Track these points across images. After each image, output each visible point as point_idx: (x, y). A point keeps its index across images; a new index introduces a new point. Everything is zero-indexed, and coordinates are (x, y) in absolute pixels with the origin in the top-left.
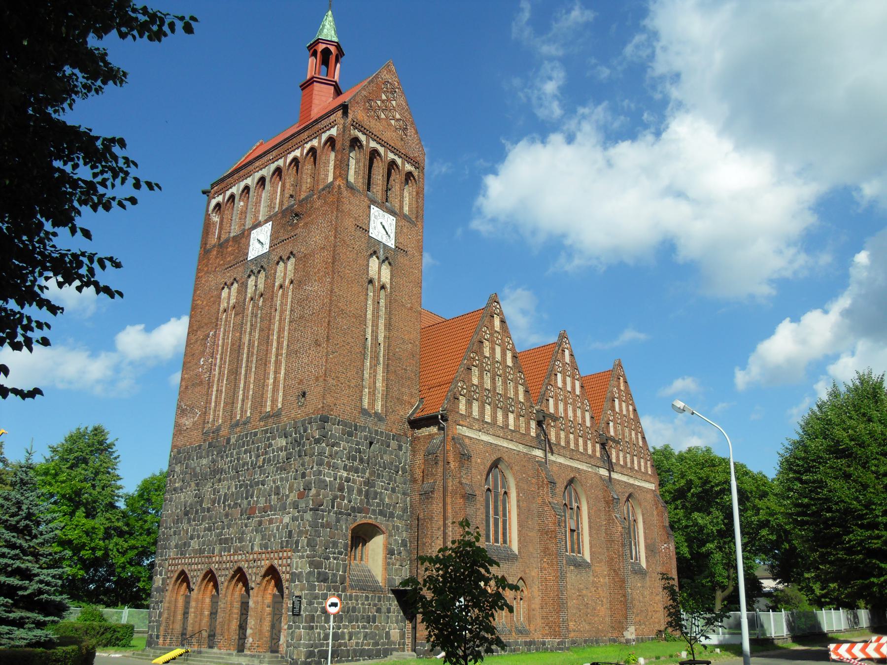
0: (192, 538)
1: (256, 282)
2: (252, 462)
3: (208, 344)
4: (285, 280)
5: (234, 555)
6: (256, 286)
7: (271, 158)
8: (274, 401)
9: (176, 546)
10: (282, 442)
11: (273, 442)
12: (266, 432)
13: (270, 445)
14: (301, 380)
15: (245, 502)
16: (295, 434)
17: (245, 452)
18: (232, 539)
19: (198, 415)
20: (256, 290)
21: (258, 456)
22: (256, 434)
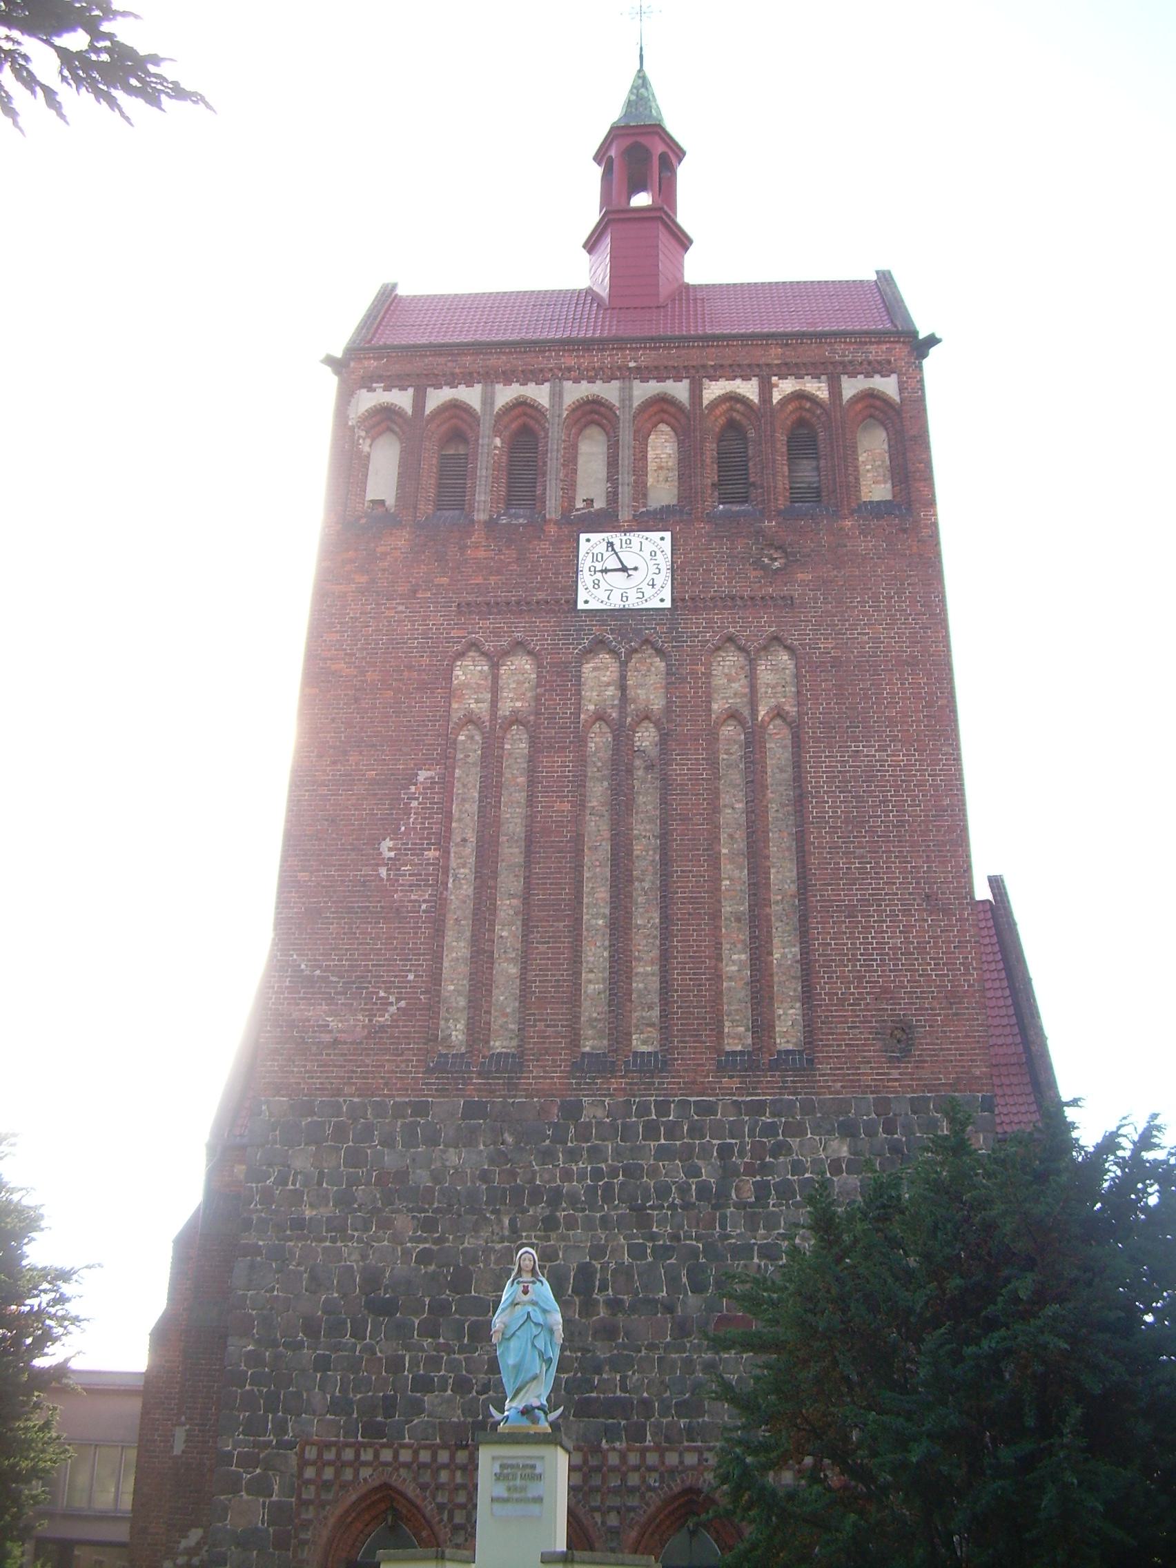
0: (424, 1385)
1: (623, 676)
2: (703, 1190)
3: (414, 804)
4: (753, 705)
5: (661, 1451)
6: (623, 688)
7: (632, 364)
8: (762, 1027)
9: (340, 1406)
10: (842, 1150)
11: (794, 1142)
12: (757, 1109)
13: (781, 1149)
14: (885, 990)
15: (693, 1299)
16: (889, 1130)
17: (662, 1153)
18: (646, 1403)
19: (393, 1009)
20: (624, 698)
21: (728, 1173)
22: (708, 1109)
